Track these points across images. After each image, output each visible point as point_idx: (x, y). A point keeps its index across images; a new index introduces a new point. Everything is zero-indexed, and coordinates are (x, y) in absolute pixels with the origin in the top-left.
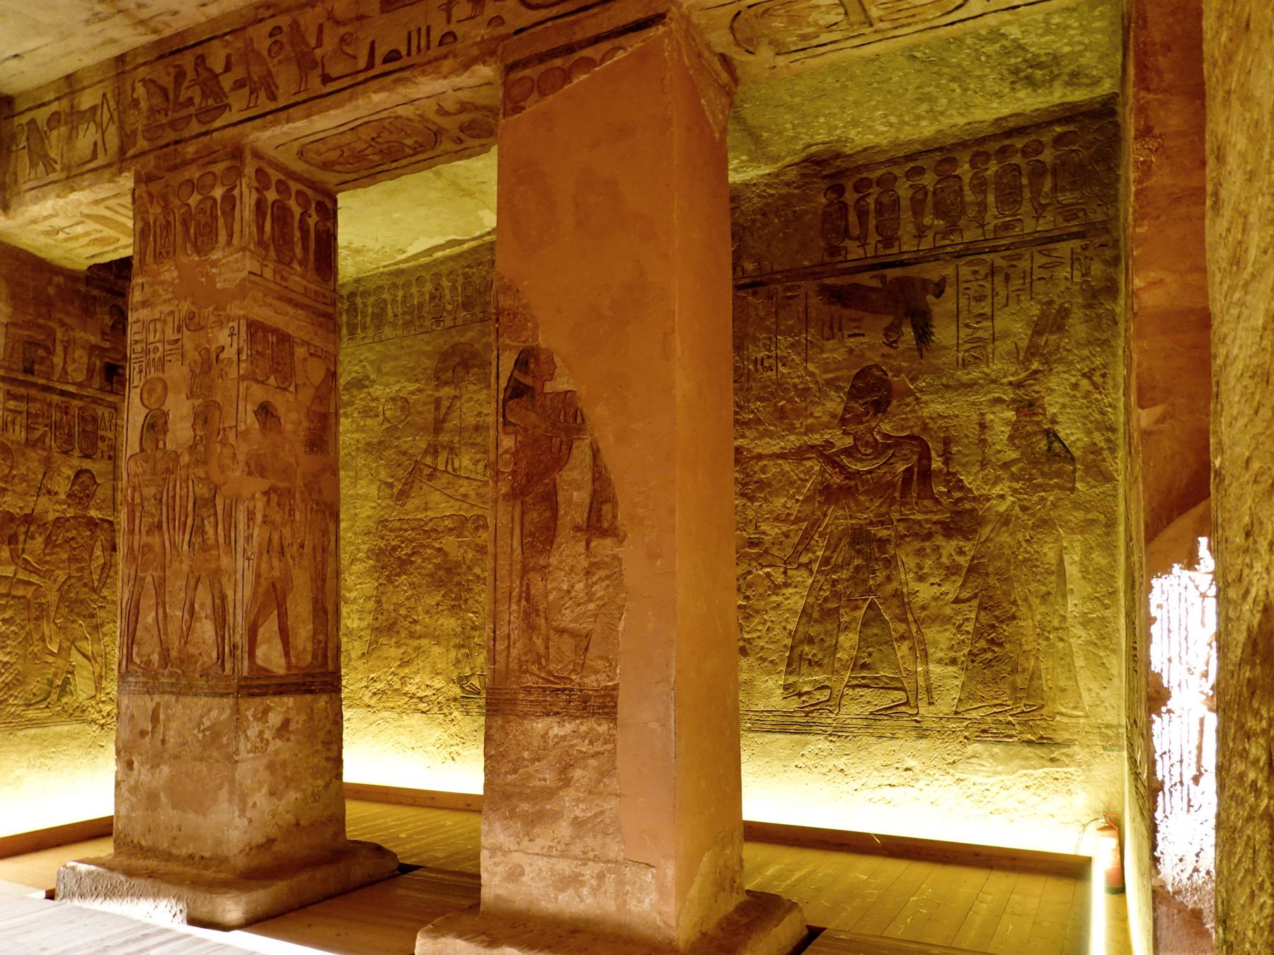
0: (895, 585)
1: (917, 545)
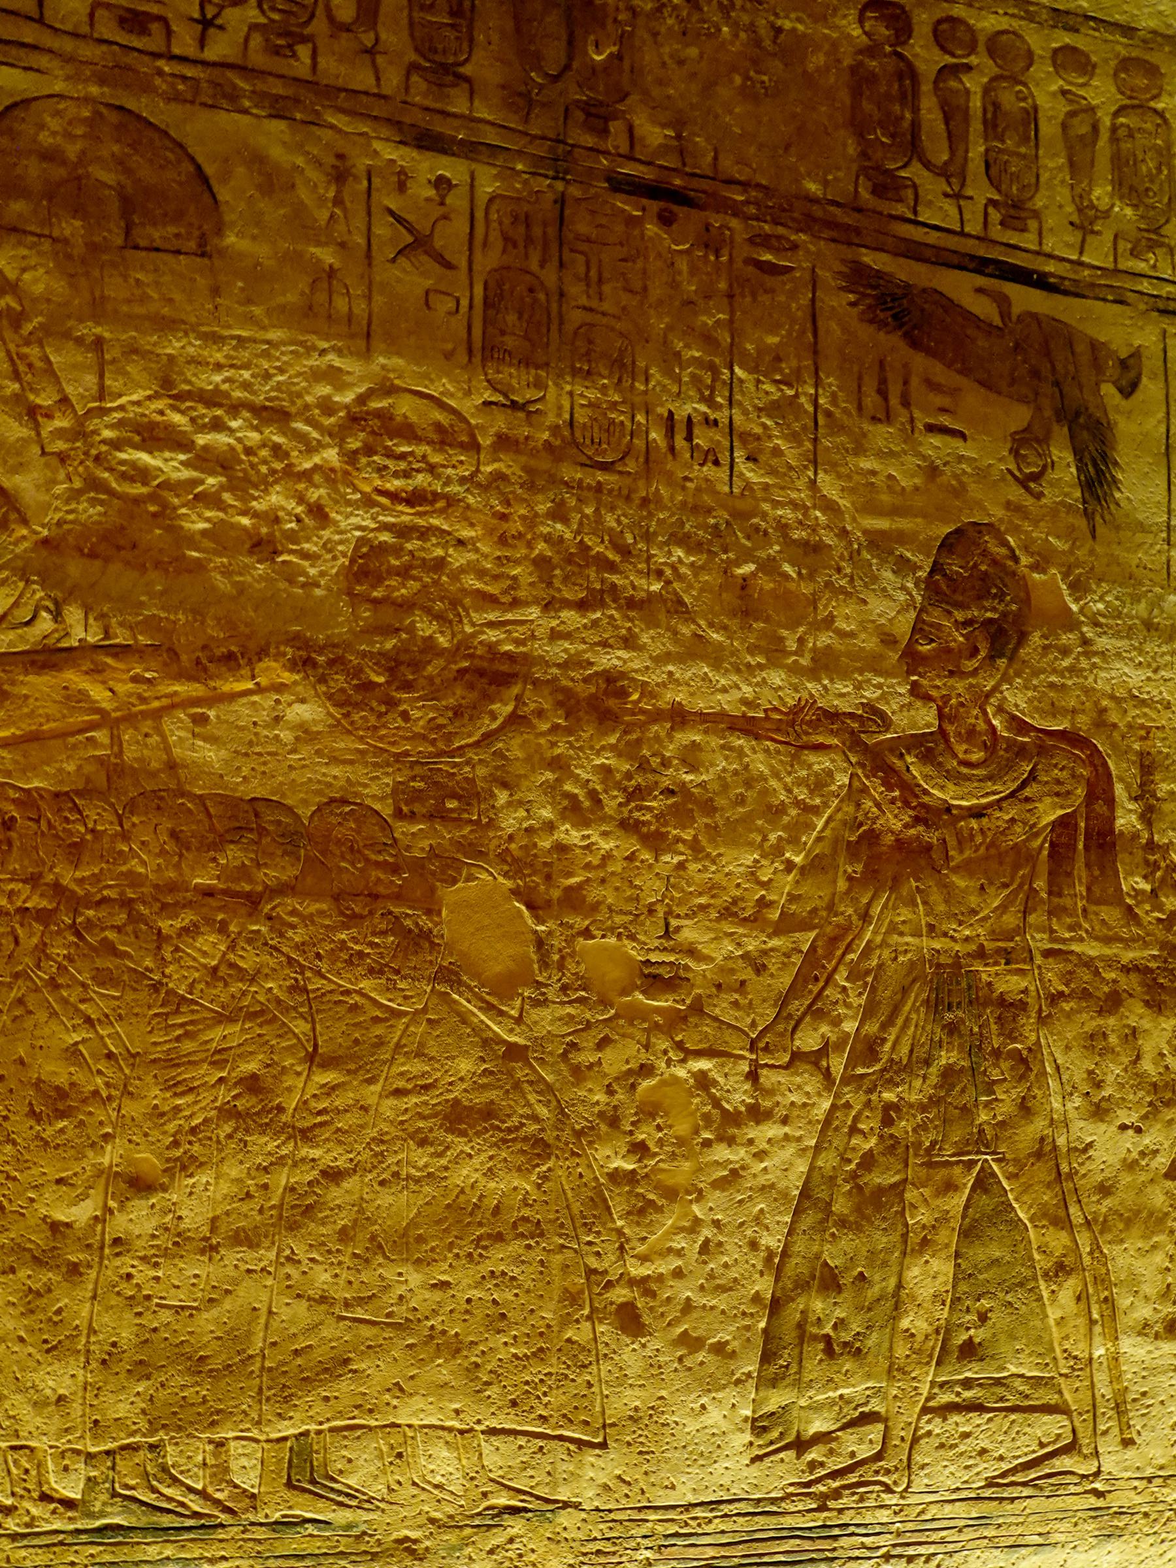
0: (1038, 1126)
1: (1090, 1022)
